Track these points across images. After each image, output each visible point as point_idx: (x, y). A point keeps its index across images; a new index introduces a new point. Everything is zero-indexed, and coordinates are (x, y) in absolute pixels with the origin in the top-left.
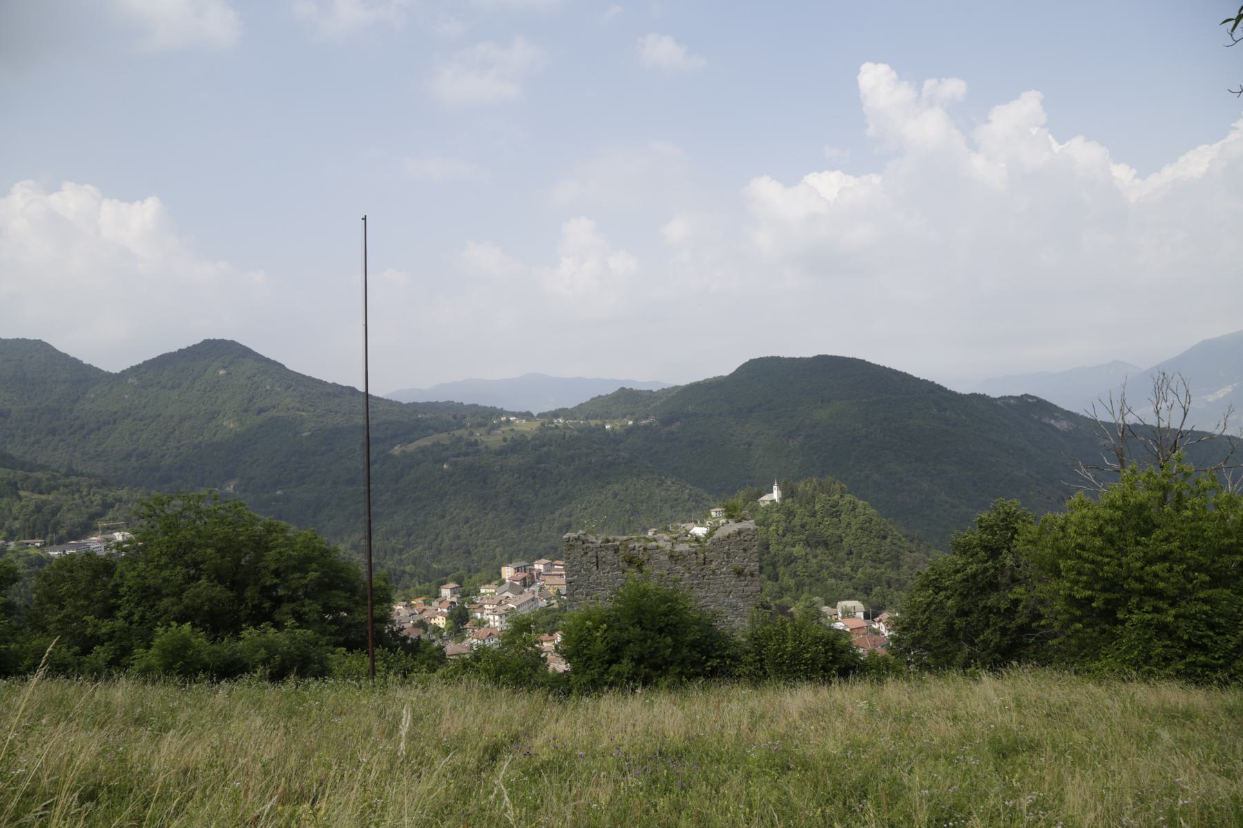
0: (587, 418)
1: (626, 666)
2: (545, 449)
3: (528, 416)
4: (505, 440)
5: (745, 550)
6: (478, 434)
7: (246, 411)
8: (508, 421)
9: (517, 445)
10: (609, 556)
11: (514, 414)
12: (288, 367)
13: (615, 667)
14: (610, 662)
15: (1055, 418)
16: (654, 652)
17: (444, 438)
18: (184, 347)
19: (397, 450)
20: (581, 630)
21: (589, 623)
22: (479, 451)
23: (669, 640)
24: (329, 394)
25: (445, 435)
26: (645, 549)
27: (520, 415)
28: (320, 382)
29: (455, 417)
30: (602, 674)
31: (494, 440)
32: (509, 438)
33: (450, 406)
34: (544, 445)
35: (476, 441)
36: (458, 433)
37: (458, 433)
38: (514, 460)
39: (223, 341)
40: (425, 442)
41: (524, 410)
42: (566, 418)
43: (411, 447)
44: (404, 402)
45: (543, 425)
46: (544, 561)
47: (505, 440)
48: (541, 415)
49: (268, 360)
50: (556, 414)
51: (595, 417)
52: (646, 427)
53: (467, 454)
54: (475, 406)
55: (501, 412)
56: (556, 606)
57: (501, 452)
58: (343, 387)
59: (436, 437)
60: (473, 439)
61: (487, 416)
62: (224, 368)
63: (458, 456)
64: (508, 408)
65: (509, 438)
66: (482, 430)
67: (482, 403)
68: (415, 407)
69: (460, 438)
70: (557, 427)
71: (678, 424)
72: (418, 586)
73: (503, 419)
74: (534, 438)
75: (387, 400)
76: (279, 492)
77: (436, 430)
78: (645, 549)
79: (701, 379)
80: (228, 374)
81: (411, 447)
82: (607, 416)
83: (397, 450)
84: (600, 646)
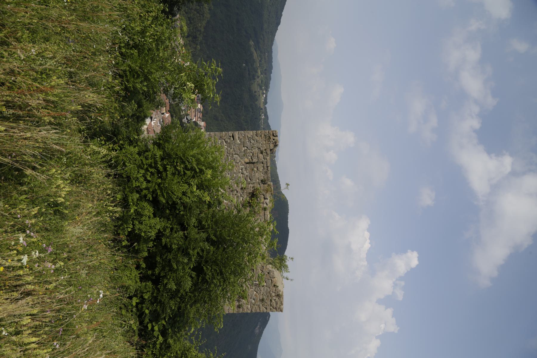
1: (151, 224)
2: (251, 110)
3: (266, 102)
4: (255, 92)
5: (262, 300)
6: (258, 80)
8: (263, 94)
9: (254, 98)
10: (259, 175)
11: (266, 96)
13: (148, 210)
14: (155, 202)
15: (260, 328)
16: (171, 266)
19: (252, 43)
20: (198, 162)
21: (209, 173)
23: (188, 284)
26: (265, 209)
27: (266, 99)
29: (265, 70)
30: (139, 190)
31: (255, 87)
32: (256, 94)
33: (271, 67)
35: (255, 79)
41: (268, 101)
42: (264, 119)
44: (273, 47)
45: (262, 109)
46: (202, 109)
47: (255, 92)
48: (265, 108)
53: (249, 74)
54: (270, 79)
55: (267, 90)
56: (182, 113)
58: (280, 19)
60: (256, 77)
65: (256, 94)
67: (271, 82)
68: (270, 52)
69: (257, 72)
70: (260, 115)
73: (264, 92)
78: (265, 209)
79: (280, 179)
81: (253, 50)
83: (252, 43)
84: (178, 188)
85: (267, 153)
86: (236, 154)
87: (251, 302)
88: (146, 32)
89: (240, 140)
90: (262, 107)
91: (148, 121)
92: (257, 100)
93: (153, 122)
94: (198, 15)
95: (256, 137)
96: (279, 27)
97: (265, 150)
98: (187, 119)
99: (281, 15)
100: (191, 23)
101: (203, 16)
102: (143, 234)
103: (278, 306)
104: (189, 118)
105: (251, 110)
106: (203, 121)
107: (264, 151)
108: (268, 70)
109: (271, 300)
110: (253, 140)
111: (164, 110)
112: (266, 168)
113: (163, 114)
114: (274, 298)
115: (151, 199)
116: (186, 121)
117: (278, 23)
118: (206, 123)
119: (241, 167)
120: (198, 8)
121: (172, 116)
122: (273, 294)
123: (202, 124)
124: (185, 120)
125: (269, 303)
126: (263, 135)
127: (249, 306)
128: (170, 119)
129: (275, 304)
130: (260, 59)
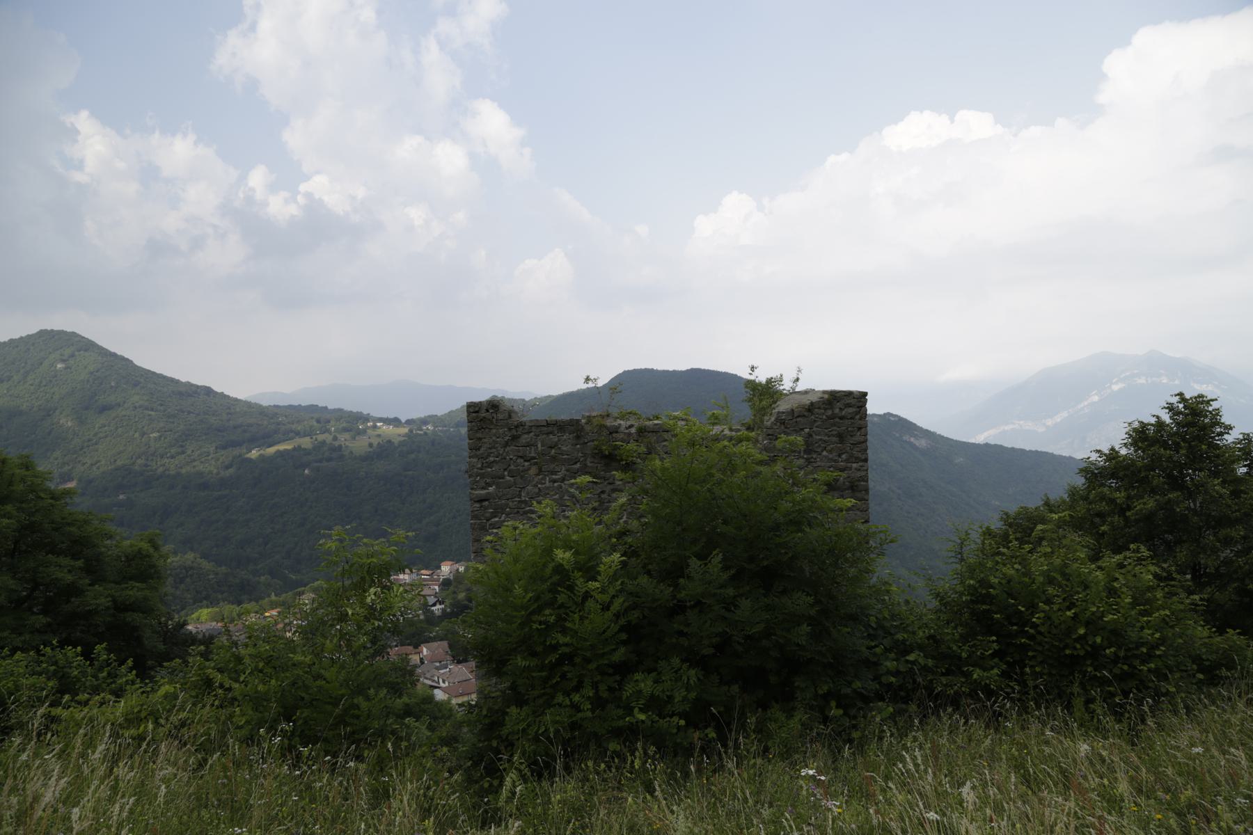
2: (413, 456)
3: (395, 422)
4: (371, 445)
5: (841, 437)
6: (343, 438)
7: (87, 408)
8: (375, 427)
9: (385, 450)
11: (381, 420)
12: (139, 362)
14: (624, 670)
15: (915, 436)
17: (306, 442)
18: (16, 336)
21: (563, 556)
24: (181, 394)
25: (307, 439)
27: (387, 421)
28: (172, 380)
29: (318, 421)
31: (359, 446)
32: (375, 444)
33: (313, 408)
35: (340, 446)
36: (321, 437)
39: (62, 333)
41: (392, 416)
43: (272, 450)
44: (265, 403)
45: (411, 431)
47: (371, 445)
48: (409, 422)
49: (114, 355)
50: (424, 421)
53: (329, 460)
54: (340, 410)
55: (365, 418)
57: (367, 458)
58: (198, 387)
60: (336, 444)
61: (354, 422)
62: (63, 361)
63: (321, 461)
64: (376, 414)
65: (375, 444)
66: (347, 435)
69: (324, 442)
70: (426, 434)
72: (273, 597)
74: (402, 444)
75: (246, 402)
76: (121, 497)
77: (298, 434)
80: (66, 368)
83: (254, 454)
85: (517, 427)
86: (520, 496)
87: (847, 461)
88: (257, 692)
89: (489, 485)
90: (405, 430)
91: (439, 695)
92: (389, 441)
93: (442, 684)
94: (188, 579)
95: (482, 451)
96: (217, 388)
97: (510, 429)
98: (434, 605)
99: (189, 384)
100: (206, 598)
101: (191, 568)
102: (693, 695)
104: (431, 600)
105: (413, 456)
106: (439, 568)
107: (514, 432)
108: (318, 417)
109: (841, 418)
110: (489, 455)
111: (415, 659)
112: (550, 429)
113: (421, 660)
114: (837, 411)
115: (618, 678)
116: (438, 606)
117: (208, 391)
118: (445, 560)
119: (548, 484)
120: (170, 580)
121: (427, 641)
122: (829, 413)
123: (446, 569)
124: (437, 609)
125: (847, 422)
126: (479, 435)
127: (854, 465)
128: (435, 644)
129: (851, 410)
130: (292, 435)
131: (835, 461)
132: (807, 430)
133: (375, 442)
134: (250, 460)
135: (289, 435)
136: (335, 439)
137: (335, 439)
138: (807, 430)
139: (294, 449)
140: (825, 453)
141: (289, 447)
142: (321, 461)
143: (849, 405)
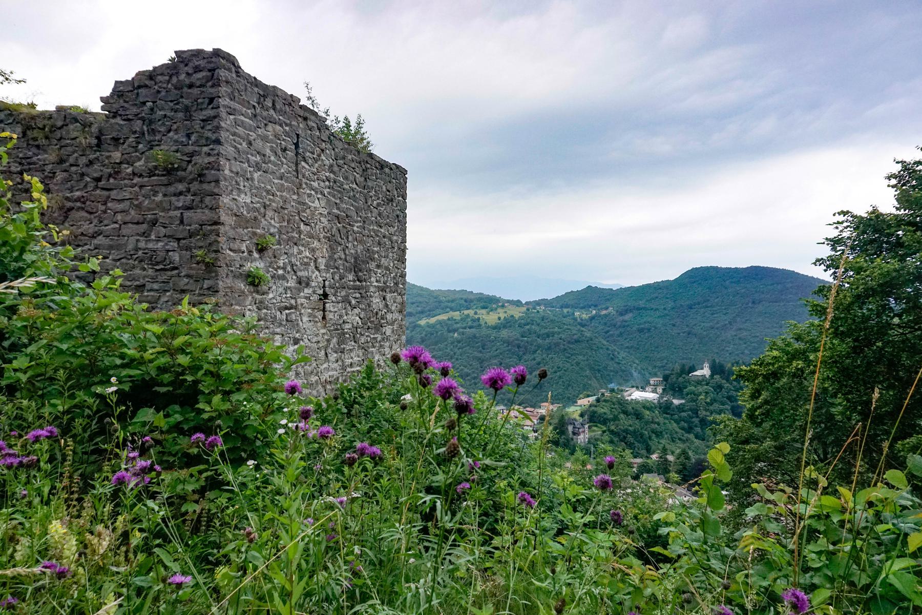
0: (562, 307)
2: (528, 327)
3: (518, 303)
4: (499, 318)
11: (508, 301)
17: (456, 315)
19: (423, 322)
22: (480, 325)
27: (511, 302)
29: (466, 301)
31: (491, 318)
34: (528, 324)
37: (466, 312)
38: (504, 333)
40: (443, 317)
41: (515, 299)
43: (433, 320)
47: (499, 318)
48: (527, 303)
50: (538, 303)
51: (567, 306)
52: (606, 316)
53: (470, 328)
57: (496, 328)
59: (452, 314)
60: (476, 317)
61: (489, 302)
63: (465, 328)
66: (484, 311)
69: (468, 316)
71: (631, 315)
74: (521, 318)
77: (452, 309)
81: (433, 320)
82: (575, 307)
83: (423, 322)
87: (196, 143)
90: (524, 309)
103: (202, 63)
114: (183, 77)
125: (195, 91)
127: (205, 149)
129: (200, 75)
131: (182, 143)
132: (149, 104)
133: (502, 316)
134: (420, 326)
135: (445, 310)
136: (476, 313)
137: (476, 313)
138: (149, 104)
139: (449, 319)
140: (171, 134)
141: (446, 318)
142: (465, 328)
143: (197, 69)
